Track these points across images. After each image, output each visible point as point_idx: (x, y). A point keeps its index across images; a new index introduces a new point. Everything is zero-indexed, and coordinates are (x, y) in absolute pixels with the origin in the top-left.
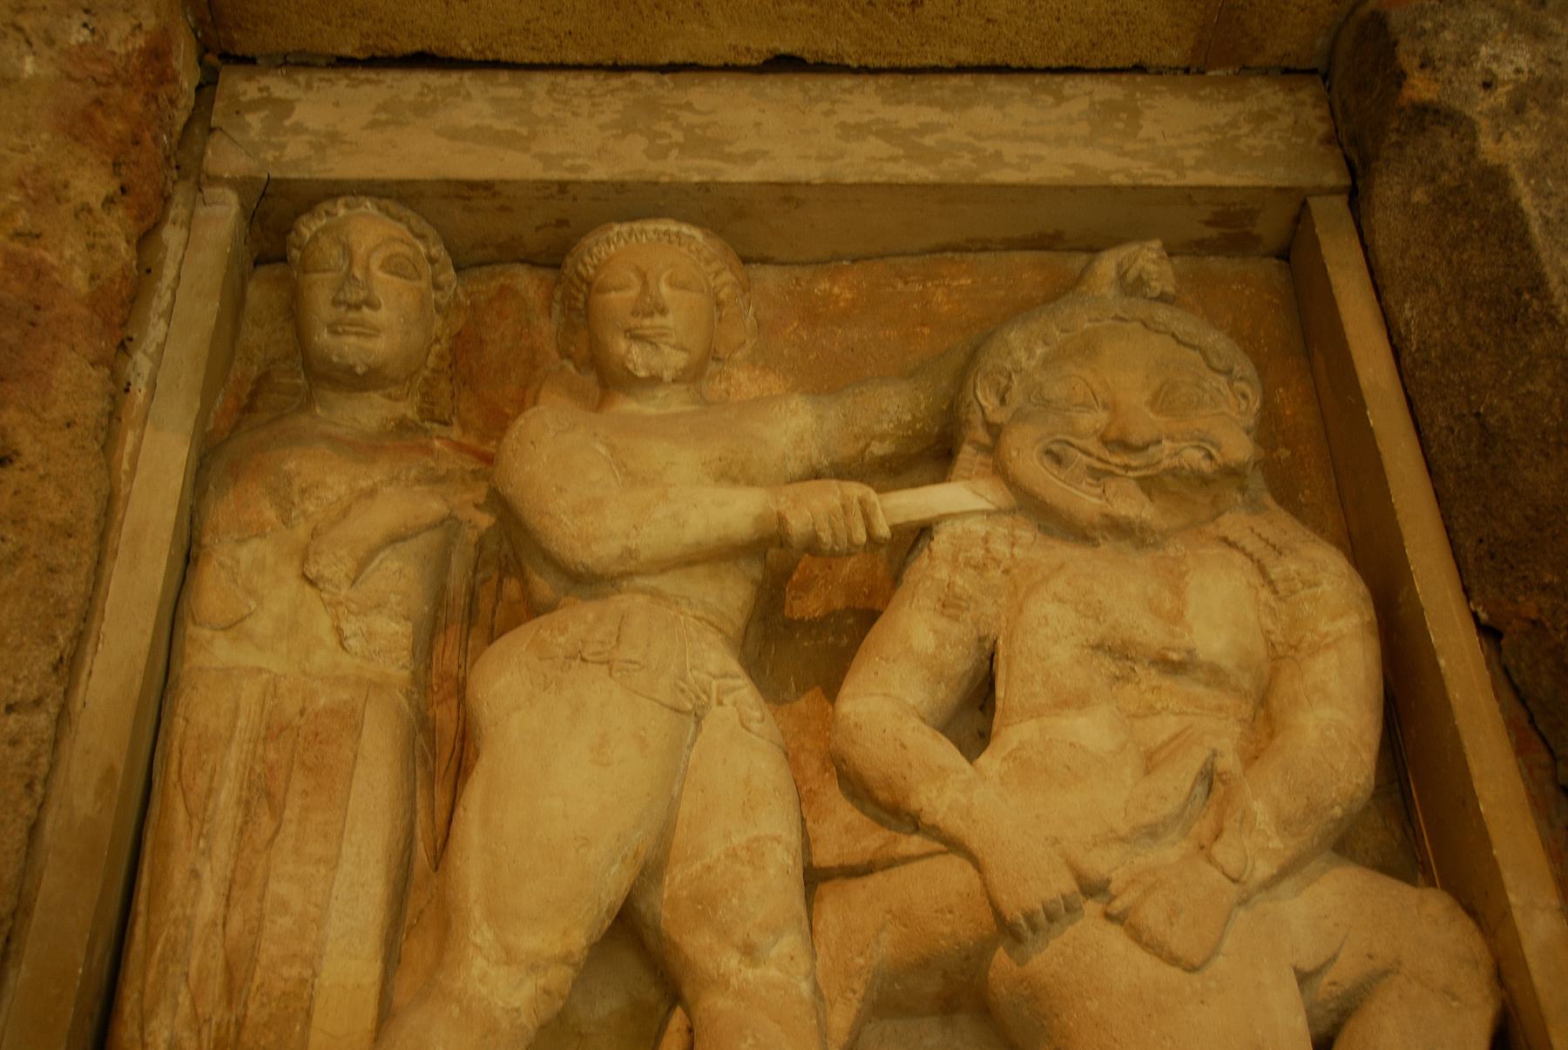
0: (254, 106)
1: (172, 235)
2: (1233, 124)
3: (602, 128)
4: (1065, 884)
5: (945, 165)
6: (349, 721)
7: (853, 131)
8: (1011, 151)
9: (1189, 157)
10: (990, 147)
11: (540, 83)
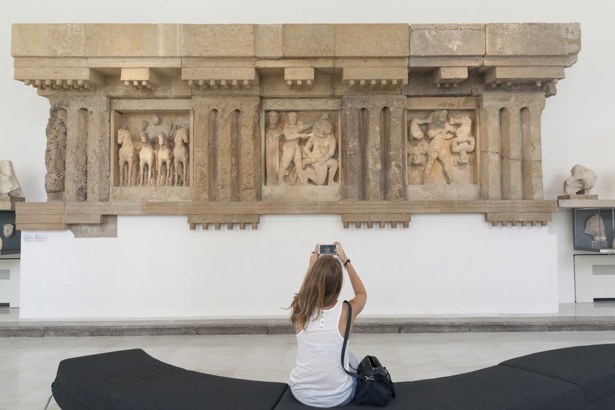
4: (315, 161)
6: (276, 149)
7: (307, 104)
11: (284, 100)
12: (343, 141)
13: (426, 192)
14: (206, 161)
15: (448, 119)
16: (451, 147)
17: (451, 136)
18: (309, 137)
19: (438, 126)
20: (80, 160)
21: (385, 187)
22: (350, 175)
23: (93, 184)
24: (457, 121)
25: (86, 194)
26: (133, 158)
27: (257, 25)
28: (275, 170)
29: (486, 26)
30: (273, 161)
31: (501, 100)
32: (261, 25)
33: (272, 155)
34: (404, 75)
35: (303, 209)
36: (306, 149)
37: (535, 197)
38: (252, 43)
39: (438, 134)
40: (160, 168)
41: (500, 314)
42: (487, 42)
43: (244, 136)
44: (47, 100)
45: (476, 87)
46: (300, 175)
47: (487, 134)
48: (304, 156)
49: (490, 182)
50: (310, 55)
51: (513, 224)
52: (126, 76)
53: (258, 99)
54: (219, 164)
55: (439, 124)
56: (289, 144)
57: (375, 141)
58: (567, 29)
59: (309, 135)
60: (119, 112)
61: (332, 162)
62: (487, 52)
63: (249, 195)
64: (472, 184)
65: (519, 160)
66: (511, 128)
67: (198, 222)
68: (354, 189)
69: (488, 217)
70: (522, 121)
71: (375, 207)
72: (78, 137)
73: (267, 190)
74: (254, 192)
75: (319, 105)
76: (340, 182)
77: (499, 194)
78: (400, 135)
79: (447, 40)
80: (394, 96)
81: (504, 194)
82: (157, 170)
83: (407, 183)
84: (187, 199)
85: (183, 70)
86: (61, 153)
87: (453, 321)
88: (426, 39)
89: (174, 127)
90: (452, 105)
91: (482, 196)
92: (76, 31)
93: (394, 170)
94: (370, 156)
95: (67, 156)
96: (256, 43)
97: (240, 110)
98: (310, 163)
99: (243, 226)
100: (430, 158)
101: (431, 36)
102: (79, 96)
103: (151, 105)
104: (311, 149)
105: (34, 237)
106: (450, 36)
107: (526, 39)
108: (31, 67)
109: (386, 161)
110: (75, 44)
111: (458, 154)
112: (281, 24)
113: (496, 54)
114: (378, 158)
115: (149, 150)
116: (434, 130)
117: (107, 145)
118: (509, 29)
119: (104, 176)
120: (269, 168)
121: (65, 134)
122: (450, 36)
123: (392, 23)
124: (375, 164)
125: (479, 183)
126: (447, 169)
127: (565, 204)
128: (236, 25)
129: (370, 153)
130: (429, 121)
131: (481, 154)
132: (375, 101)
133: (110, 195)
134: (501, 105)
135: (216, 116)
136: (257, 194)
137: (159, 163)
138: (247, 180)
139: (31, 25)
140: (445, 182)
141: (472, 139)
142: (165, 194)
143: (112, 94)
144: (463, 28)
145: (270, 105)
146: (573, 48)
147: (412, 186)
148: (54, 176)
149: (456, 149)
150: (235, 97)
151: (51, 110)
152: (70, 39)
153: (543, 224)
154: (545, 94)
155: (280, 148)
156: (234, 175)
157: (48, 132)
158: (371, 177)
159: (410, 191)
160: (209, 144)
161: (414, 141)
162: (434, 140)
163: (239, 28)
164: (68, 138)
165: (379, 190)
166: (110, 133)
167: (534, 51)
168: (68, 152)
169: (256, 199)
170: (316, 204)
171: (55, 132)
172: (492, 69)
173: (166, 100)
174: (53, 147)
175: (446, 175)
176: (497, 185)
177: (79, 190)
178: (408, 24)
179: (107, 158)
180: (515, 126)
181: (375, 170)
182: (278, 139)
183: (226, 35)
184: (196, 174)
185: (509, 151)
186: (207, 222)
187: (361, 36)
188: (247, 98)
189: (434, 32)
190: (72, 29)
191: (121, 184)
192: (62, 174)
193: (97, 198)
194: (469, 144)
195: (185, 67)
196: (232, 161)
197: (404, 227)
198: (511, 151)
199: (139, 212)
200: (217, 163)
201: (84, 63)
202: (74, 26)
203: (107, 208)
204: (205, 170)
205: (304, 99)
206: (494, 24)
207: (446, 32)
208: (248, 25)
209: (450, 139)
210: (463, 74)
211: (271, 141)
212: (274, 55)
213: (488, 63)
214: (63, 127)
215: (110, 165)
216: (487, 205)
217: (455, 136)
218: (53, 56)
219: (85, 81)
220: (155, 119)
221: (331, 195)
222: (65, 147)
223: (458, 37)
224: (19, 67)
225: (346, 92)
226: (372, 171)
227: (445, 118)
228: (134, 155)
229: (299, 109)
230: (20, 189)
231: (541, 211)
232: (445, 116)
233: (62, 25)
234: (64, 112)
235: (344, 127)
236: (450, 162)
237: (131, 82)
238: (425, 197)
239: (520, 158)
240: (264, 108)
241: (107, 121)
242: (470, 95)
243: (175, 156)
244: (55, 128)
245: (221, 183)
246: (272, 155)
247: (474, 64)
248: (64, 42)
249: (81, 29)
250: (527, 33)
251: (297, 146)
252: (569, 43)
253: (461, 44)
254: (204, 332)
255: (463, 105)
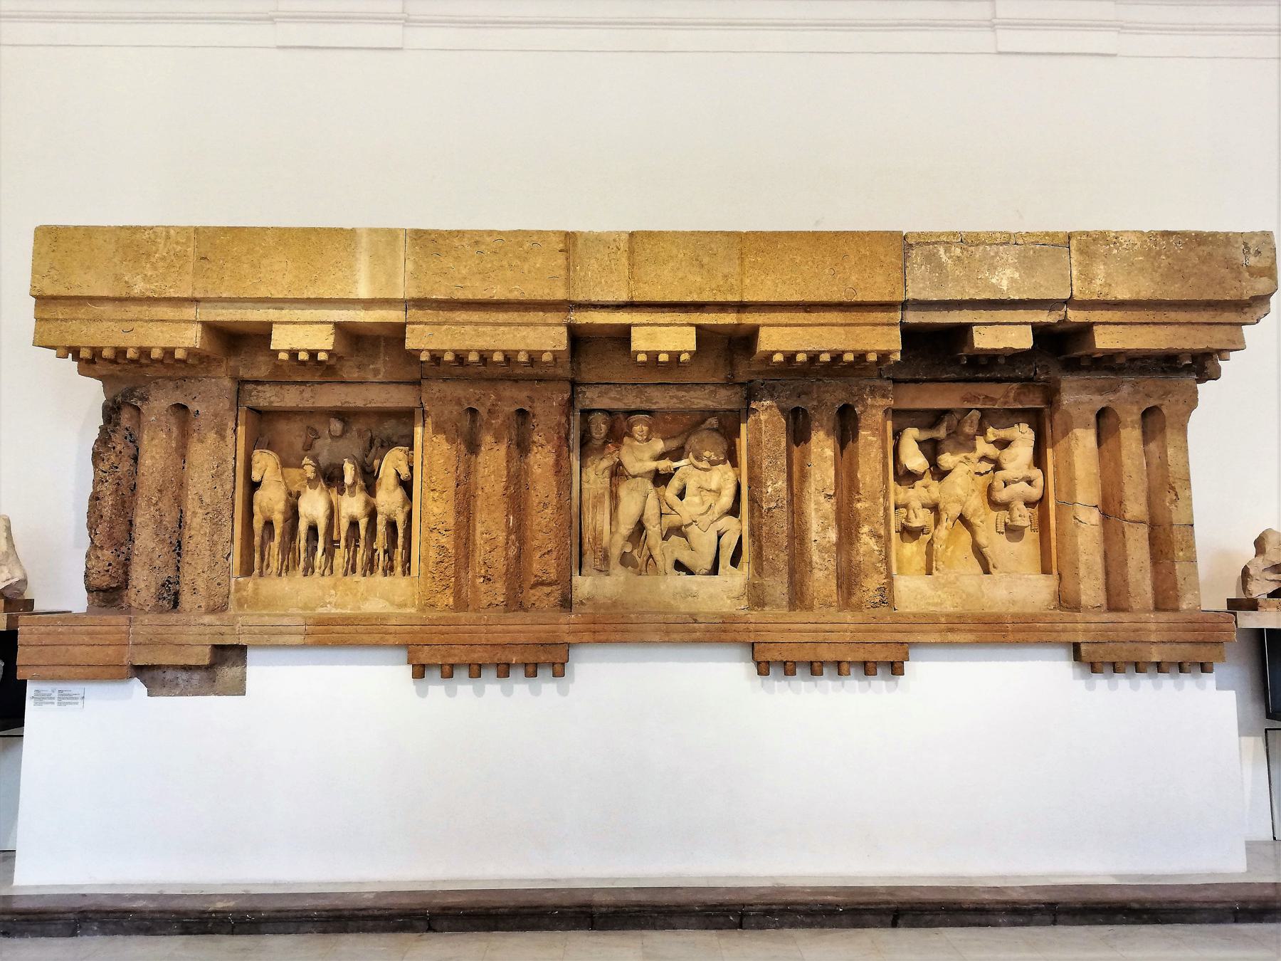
0: (580, 393)
1: (571, 418)
2: (731, 395)
3: (633, 397)
5: (685, 404)
6: (603, 495)
7: (672, 397)
8: (696, 401)
9: (723, 402)
10: (692, 400)
11: (623, 387)
12: (750, 479)
13: (939, 593)
14: (451, 521)
15: (982, 432)
16: (990, 489)
17: (989, 466)
18: (676, 469)
19: (961, 444)
20: (166, 522)
21: (848, 580)
22: (768, 553)
23: (196, 573)
24: (1003, 434)
25: (177, 594)
26: (284, 513)
27: (573, 233)
28: (602, 540)
29: (1070, 236)
30: (598, 520)
31: (1101, 391)
32: (582, 233)
33: (595, 507)
34: (891, 341)
35: (667, 632)
36: (670, 492)
37: (1184, 607)
38: (563, 272)
39: (961, 462)
40: (343, 535)
41: (1115, 876)
42: (1075, 273)
43: (536, 467)
44: (97, 385)
45: (1043, 363)
46: (656, 553)
47: (1070, 465)
48: (665, 509)
49: (1082, 571)
50: (689, 299)
51: (1139, 667)
52: (282, 340)
53: (568, 386)
54: (479, 528)
55: (967, 444)
56: (632, 483)
57: (824, 480)
58: (1245, 244)
59: (676, 464)
60: (254, 410)
61: (729, 523)
62: (1074, 293)
63: (544, 598)
65: (1144, 523)
66: (1124, 453)
67: (430, 662)
68: (778, 587)
69: (1083, 654)
70: (1147, 437)
71: (828, 627)
72: (164, 470)
73: (584, 585)
74: (556, 592)
75: (700, 400)
76: (746, 568)
77: (1102, 599)
78: (879, 467)
79: (986, 267)
80: (865, 382)
81: (1115, 600)
82: (335, 537)
83: (894, 571)
84: (406, 605)
85: (408, 328)
86: (123, 502)
87: (1015, 896)
88: (940, 266)
89: (377, 442)
91: (1066, 601)
92: (177, 243)
93: (867, 543)
94: (813, 513)
95: (140, 512)
96: (571, 273)
97: (527, 409)
98: (678, 524)
99: (531, 670)
100: (944, 516)
101: (950, 257)
102: (170, 379)
103: (332, 397)
104: (681, 495)
105: (56, 695)
106: (993, 257)
107: (1159, 267)
108: (72, 320)
109: (847, 525)
110: (173, 270)
111: (1006, 506)
112: (626, 232)
113: (1095, 297)
114: (832, 516)
115: (320, 494)
116: (952, 454)
117: (229, 486)
118: (1121, 244)
119: (218, 556)
120: (588, 536)
121: (135, 459)
122: (993, 257)
123: (867, 229)
124: (825, 529)
125: (1055, 571)
126: (982, 539)
127: (1250, 621)
128: (527, 234)
129: (813, 506)
130: (941, 433)
132: (824, 392)
133: (231, 597)
134: (1099, 402)
135: (473, 421)
136: (563, 595)
137: (344, 525)
138: (542, 565)
139: (76, 228)
140: (979, 569)
141: (1036, 474)
142: (355, 595)
143: (244, 373)
144: (1020, 241)
145: (593, 398)
146: (1261, 286)
147: (907, 578)
148: (107, 554)
149: (1002, 495)
150: (516, 381)
151: (105, 407)
152: (163, 259)
153: (1205, 668)
154: (1195, 377)
155: (611, 491)
156: (513, 552)
157: (97, 457)
158: (816, 558)
159: (902, 588)
160: (458, 485)
161: (907, 477)
163: (535, 238)
164: (142, 470)
165: (835, 588)
166: (235, 458)
167: (1175, 291)
168: (142, 502)
169: (561, 605)
170: (696, 621)
171: (113, 457)
172: (1085, 330)
173: (363, 387)
174: (107, 489)
175: (982, 553)
176: (1097, 579)
177: (163, 585)
178: (901, 232)
179: (227, 514)
180: (1134, 446)
181: (824, 543)
182: (607, 473)
183: (506, 254)
184: (427, 550)
185: (1121, 503)
186: (451, 661)
187: (798, 259)
188: (543, 384)
189: (958, 250)
190: (168, 237)
191: (257, 571)
192: (124, 549)
193: (203, 604)
195: (413, 323)
196: (508, 521)
197: (892, 674)
198: (1127, 503)
199: (298, 639)
200: (474, 526)
201: (190, 312)
202: (172, 232)
203: (224, 629)
204: (447, 541)
205: (666, 386)
206: (1087, 234)
207: (985, 250)
208: (554, 232)
209: (987, 472)
210: (1022, 339)
211: (592, 476)
212: (609, 298)
213: (1075, 316)
214: (130, 444)
215: (232, 530)
216: (1079, 626)
217: (998, 467)
218: (124, 295)
219: (190, 352)
220: (336, 426)
221: (725, 597)
222: (134, 488)
223: (1010, 261)
224: (47, 320)
225: (759, 373)
226: (818, 546)
227: (976, 427)
228: (286, 506)
229: (654, 407)
230: (24, 581)
231: (1200, 638)
232: (976, 422)
233: (145, 228)
234: (134, 413)
235: (754, 446)
236: (988, 525)
237: (293, 354)
238: (936, 605)
239: (1146, 518)
240: (579, 406)
241: (229, 432)
242: (1031, 380)
243: (380, 509)
244: (114, 448)
245: (483, 571)
246: (595, 507)
247: (1044, 317)
248: (148, 265)
249: (188, 238)
250: (1159, 254)
251: (650, 486)
252: (1252, 275)
253: (1017, 275)
254: (445, 923)
255: (1015, 400)
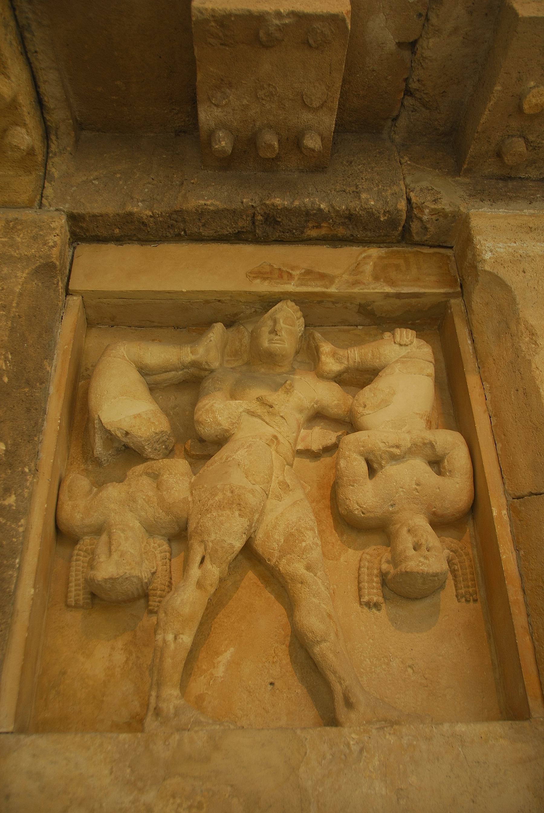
45: (424, 184)
64: (489, 719)
90: (322, 276)
131: (513, 510)
162: (224, 452)
194: (439, 473)
